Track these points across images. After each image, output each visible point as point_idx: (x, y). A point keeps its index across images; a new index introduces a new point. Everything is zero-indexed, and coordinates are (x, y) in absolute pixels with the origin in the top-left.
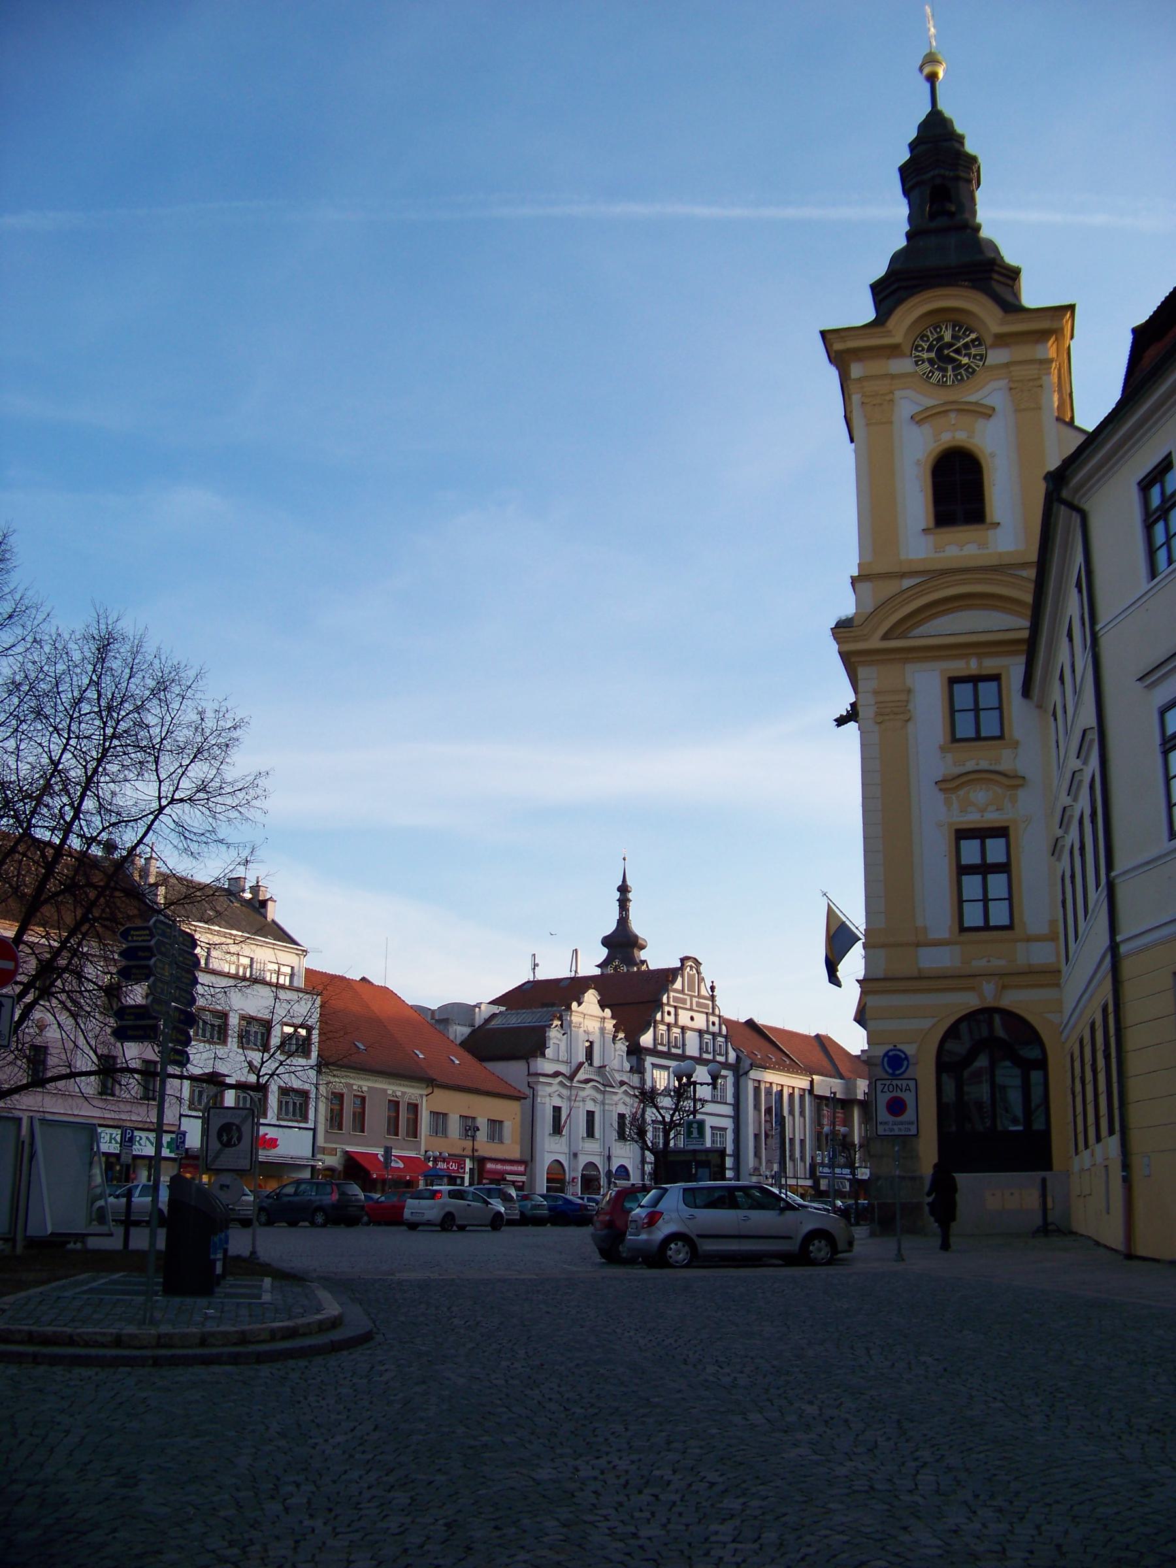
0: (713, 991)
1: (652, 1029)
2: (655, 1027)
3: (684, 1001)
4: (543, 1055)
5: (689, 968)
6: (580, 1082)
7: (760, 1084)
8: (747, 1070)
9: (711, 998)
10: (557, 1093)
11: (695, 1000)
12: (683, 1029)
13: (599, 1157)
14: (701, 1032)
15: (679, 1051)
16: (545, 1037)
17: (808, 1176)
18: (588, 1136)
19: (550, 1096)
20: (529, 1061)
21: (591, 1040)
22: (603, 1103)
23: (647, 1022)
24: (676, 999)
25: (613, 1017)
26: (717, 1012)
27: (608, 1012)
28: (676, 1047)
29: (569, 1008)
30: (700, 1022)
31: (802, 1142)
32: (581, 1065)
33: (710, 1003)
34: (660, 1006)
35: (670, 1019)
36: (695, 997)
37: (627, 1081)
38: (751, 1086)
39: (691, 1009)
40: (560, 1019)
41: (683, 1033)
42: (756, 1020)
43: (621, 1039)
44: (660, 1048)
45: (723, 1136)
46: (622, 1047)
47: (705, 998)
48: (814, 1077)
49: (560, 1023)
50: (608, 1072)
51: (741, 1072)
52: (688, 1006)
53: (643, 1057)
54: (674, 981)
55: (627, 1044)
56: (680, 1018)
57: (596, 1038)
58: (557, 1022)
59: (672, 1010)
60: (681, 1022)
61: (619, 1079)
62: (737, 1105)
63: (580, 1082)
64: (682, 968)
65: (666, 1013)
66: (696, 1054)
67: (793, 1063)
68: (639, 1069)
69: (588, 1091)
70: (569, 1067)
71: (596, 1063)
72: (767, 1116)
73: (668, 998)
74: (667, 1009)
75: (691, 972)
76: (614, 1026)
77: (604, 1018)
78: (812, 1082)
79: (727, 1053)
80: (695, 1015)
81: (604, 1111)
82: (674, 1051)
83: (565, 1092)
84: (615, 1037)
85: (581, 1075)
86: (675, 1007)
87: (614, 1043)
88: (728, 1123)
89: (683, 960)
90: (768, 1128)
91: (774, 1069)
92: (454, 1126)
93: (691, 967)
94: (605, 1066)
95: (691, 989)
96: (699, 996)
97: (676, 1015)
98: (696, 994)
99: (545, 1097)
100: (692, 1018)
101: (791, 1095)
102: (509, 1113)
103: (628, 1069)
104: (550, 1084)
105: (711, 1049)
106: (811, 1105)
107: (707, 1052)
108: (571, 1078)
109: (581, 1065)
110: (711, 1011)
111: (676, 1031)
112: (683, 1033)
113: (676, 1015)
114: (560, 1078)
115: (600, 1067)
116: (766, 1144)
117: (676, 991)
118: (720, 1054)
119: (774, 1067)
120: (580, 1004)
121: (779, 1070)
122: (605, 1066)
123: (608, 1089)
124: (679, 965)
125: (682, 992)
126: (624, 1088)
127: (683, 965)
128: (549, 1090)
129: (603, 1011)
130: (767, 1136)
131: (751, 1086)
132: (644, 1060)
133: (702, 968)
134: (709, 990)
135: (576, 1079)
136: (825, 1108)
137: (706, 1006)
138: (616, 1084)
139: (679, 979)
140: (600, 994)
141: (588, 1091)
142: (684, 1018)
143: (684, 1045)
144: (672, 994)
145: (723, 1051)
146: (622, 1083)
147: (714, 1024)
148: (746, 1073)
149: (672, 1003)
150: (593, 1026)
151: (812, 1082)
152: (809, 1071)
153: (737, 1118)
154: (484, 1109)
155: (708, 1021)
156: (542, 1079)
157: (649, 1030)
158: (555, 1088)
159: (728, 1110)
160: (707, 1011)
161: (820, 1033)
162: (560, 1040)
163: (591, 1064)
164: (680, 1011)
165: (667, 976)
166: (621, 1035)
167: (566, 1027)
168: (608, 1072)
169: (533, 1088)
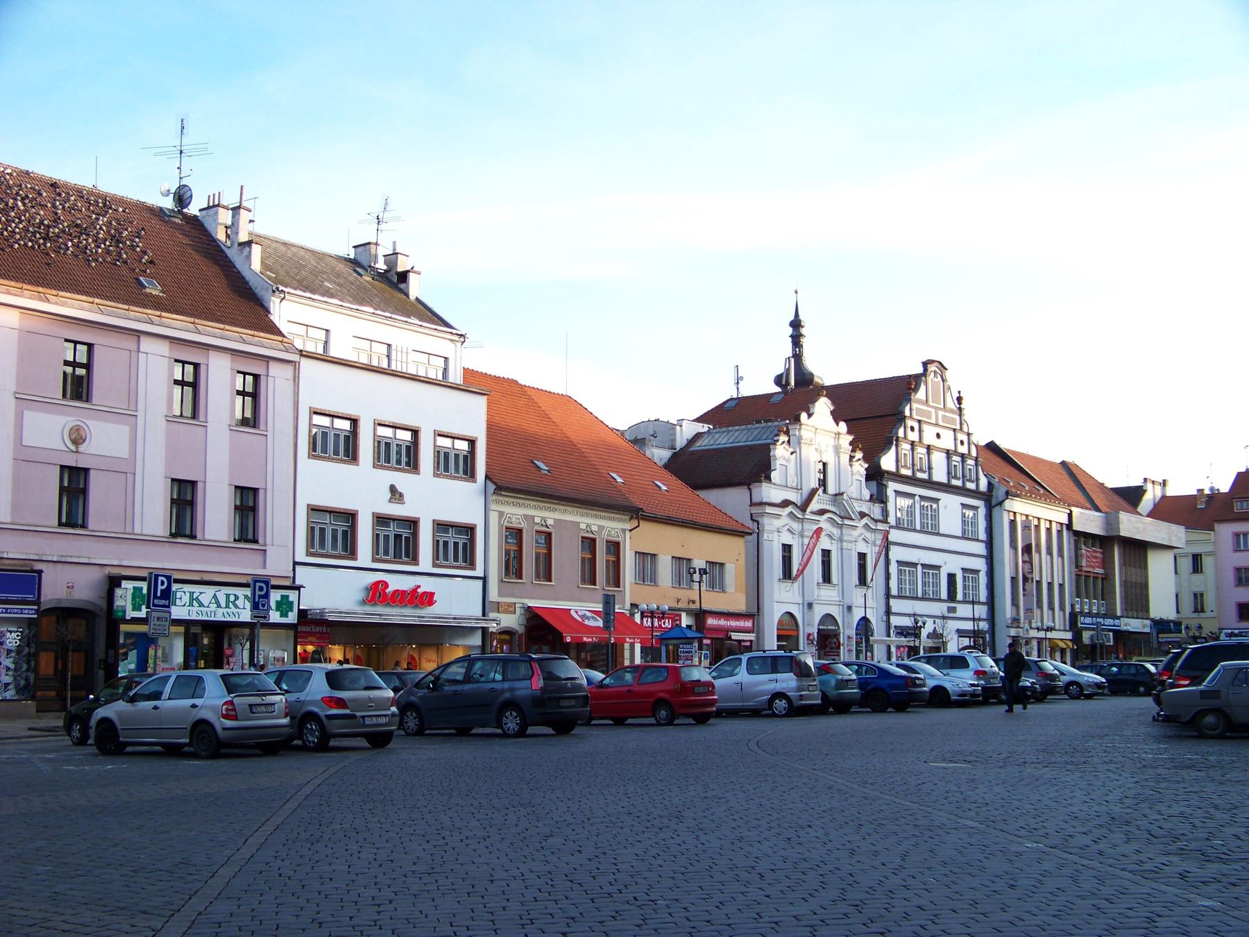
0: (960, 403)
1: (894, 448)
2: (897, 446)
3: (928, 415)
4: (768, 478)
5: (932, 374)
6: (812, 513)
8: (1001, 499)
9: (958, 411)
10: (787, 527)
11: (941, 413)
12: (928, 448)
13: (838, 607)
14: (948, 453)
15: (925, 476)
16: (770, 457)
17: (1068, 628)
18: (824, 581)
20: (751, 487)
21: (824, 461)
22: (841, 540)
23: (888, 441)
24: (919, 411)
25: (849, 432)
26: (966, 430)
27: (843, 426)
28: (921, 470)
29: (797, 420)
30: (947, 441)
31: (1061, 586)
32: (813, 492)
33: (957, 418)
34: (901, 419)
35: (913, 436)
36: (940, 409)
37: (867, 513)
38: (1006, 518)
39: (937, 425)
40: (787, 433)
41: (929, 453)
42: (998, 443)
43: (859, 459)
44: (904, 472)
45: (976, 580)
46: (860, 468)
47: (951, 411)
48: (1074, 509)
49: (787, 439)
51: (994, 502)
52: (934, 421)
53: (884, 482)
54: (916, 389)
55: (866, 466)
56: (925, 435)
57: (830, 458)
58: (783, 438)
59: (916, 425)
60: (926, 441)
61: (859, 510)
62: (990, 543)
63: (812, 513)
64: (925, 373)
65: (909, 429)
66: (945, 480)
67: (1048, 493)
68: (879, 498)
70: (799, 495)
71: (832, 489)
72: (1026, 555)
73: (911, 409)
74: (909, 423)
75: (935, 379)
76: (851, 443)
77: (839, 434)
78: (1070, 515)
79: (978, 479)
80: (941, 431)
81: (842, 549)
82: (919, 475)
83: (796, 526)
84: (851, 458)
85: (815, 505)
86: (919, 422)
87: (851, 465)
88: (980, 564)
89: (925, 364)
90: (1027, 570)
91: (1026, 497)
94: (842, 494)
97: (920, 431)
98: (942, 407)
99: (772, 532)
100: (938, 436)
101: (1049, 530)
102: (730, 551)
103: (868, 497)
105: (960, 474)
106: (1069, 543)
107: (956, 477)
108: (803, 507)
109: (813, 492)
111: (921, 451)
112: (929, 453)
113: (920, 431)
114: (790, 509)
115: (836, 495)
116: (1024, 590)
117: (919, 402)
118: (970, 480)
119: (1031, 496)
120: (810, 415)
121: (1030, 498)
122: (842, 494)
123: (846, 522)
124: (920, 370)
126: (865, 520)
127: (925, 370)
128: (777, 523)
129: (838, 425)
130: (1025, 579)
131: (1006, 518)
132: (886, 487)
133: (948, 374)
134: (956, 402)
135: (809, 510)
136: (1083, 547)
138: (855, 515)
139: (923, 387)
140: (834, 403)
142: (929, 437)
143: (930, 468)
144: (915, 406)
145: (973, 477)
146: (863, 515)
147: (962, 443)
148: (1001, 503)
149: (915, 416)
150: (826, 442)
151: (1070, 515)
152: (1067, 503)
153: (990, 558)
155: (955, 439)
156: (769, 510)
157: (890, 448)
158: (785, 520)
159: (980, 548)
160: (954, 427)
161: (1066, 460)
162: (788, 460)
163: (825, 491)
164: (925, 427)
165: (910, 383)
166: (859, 455)
167: (795, 444)
169: (758, 522)
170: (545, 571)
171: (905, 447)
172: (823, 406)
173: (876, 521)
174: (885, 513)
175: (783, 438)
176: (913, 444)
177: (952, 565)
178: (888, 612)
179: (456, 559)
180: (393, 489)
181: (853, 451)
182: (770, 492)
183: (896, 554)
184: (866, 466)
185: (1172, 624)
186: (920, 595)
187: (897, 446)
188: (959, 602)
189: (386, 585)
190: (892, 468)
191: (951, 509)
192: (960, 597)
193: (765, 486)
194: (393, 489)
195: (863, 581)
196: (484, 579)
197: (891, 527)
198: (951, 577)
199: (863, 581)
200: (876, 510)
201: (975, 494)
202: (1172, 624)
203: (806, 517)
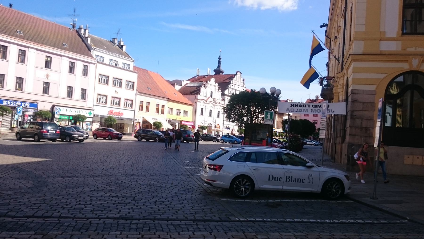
2: (229, 89)
3: (237, 83)
19: (200, 105)
24: (235, 82)
25: (218, 85)
46: (220, 93)
59: (233, 85)
60: (235, 89)
74: (232, 84)
76: (218, 88)
83: (205, 105)
84: (218, 91)
85: (209, 100)
89: (237, 72)
92: (174, 111)
95: (238, 80)
97: (234, 87)
102: (190, 109)
104: (201, 102)
114: (203, 101)
122: (215, 98)
123: (216, 104)
124: (236, 73)
135: (207, 101)
154: (183, 108)
166: (220, 91)
170: (148, 109)
173: (222, 105)
174: (224, 103)
176: (232, 89)
179: (129, 106)
180: (116, 91)
181: (219, 89)
187: (229, 89)
190: (227, 94)
194: (116, 91)
196: (135, 111)
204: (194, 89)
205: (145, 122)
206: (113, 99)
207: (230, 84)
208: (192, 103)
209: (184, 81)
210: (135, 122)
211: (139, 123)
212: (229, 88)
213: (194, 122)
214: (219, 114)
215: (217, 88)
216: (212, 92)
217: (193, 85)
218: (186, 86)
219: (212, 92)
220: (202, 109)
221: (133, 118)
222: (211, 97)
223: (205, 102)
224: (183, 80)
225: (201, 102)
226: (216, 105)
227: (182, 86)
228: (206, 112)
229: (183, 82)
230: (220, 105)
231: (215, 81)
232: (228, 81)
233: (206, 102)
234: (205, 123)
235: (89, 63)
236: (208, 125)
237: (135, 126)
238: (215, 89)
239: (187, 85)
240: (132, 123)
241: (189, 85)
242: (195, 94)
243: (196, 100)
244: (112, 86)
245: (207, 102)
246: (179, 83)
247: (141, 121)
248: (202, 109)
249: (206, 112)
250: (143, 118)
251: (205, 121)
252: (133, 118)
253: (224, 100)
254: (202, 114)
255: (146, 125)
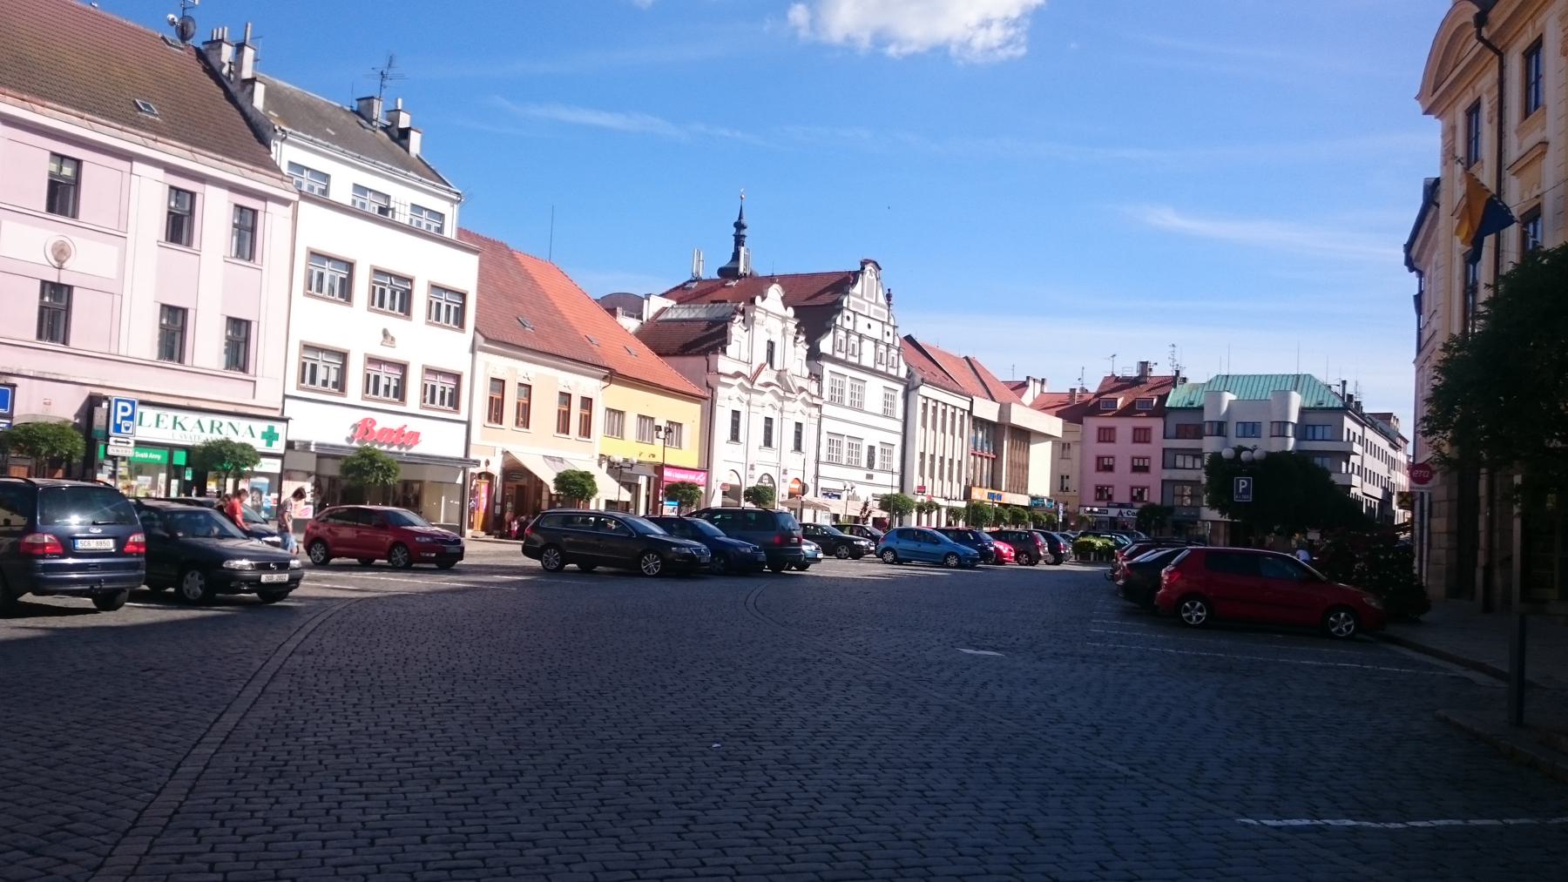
1: (831, 335)
2: (834, 333)
4: (724, 351)
6: (760, 385)
7: (937, 404)
11: (873, 307)
17: (962, 498)
18: (765, 445)
19: (728, 399)
25: (796, 316)
27: (791, 312)
29: (753, 301)
33: (886, 312)
35: (849, 325)
37: (806, 388)
38: (920, 401)
39: (869, 317)
40: (743, 313)
46: (802, 350)
49: (742, 318)
50: (789, 376)
54: (855, 282)
55: (807, 347)
56: (858, 324)
58: (739, 317)
63: (760, 385)
66: (871, 365)
68: (816, 377)
69: (769, 398)
71: (777, 365)
74: (846, 313)
75: (870, 277)
76: (796, 326)
80: (872, 323)
83: (746, 397)
84: (796, 338)
85: (762, 379)
86: (855, 313)
93: (870, 271)
94: (786, 370)
96: (876, 303)
98: (874, 301)
110: (886, 320)
111: (854, 339)
113: (855, 321)
114: (740, 380)
117: (856, 296)
120: (764, 298)
122: (786, 370)
123: (788, 395)
125: (861, 297)
126: (804, 394)
135: (756, 382)
137: (882, 314)
139: (860, 282)
141: (769, 398)
144: (852, 298)
146: (802, 390)
148: (918, 387)
156: (723, 379)
159: (898, 427)
163: (772, 366)
164: (858, 317)
166: (802, 338)
167: (748, 323)
168: (789, 376)
169: (713, 389)
171: (841, 334)
172: (775, 292)
174: (820, 390)
175: (739, 317)
177: (872, 438)
178: (817, 476)
181: (798, 333)
182: (724, 364)
183: (827, 425)
184: (807, 347)
185: (1045, 500)
186: (844, 462)
188: (877, 471)
189: (373, 422)
190: (830, 352)
191: (875, 389)
192: (877, 466)
193: (721, 358)
195: (798, 447)
197: (825, 402)
198: (872, 448)
199: (798, 447)
200: (813, 387)
201: (897, 379)
202: (1045, 500)
203: (754, 388)
204: (697, 332)
205: (515, 472)
206: (374, 370)
207: (839, 310)
208: (696, 391)
209: (652, 298)
210: (472, 474)
211: (489, 476)
212: (835, 327)
213: (706, 468)
214: (798, 435)
215: (791, 326)
216: (771, 344)
217: (692, 316)
218: (659, 321)
219: (771, 344)
220: (736, 414)
221: (461, 455)
222: (768, 365)
223: (749, 386)
224: (648, 297)
225: (731, 386)
226: (789, 399)
227: (645, 319)
228: (753, 429)
229: (646, 302)
230: (804, 400)
231: (783, 298)
232: (827, 298)
233: (753, 383)
234: (749, 472)
235: (264, 197)
236: (761, 480)
237: (474, 493)
238: (784, 331)
239: (662, 317)
240: (460, 481)
241: (671, 315)
242: (705, 353)
243: (711, 378)
244: (370, 310)
245: (756, 387)
246: (634, 306)
247: (496, 469)
248: (736, 414)
249: (753, 429)
250: (506, 453)
251: (748, 467)
252: (461, 455)
253: (817, 376)
254: (735, 437)
255: (518, 486)
